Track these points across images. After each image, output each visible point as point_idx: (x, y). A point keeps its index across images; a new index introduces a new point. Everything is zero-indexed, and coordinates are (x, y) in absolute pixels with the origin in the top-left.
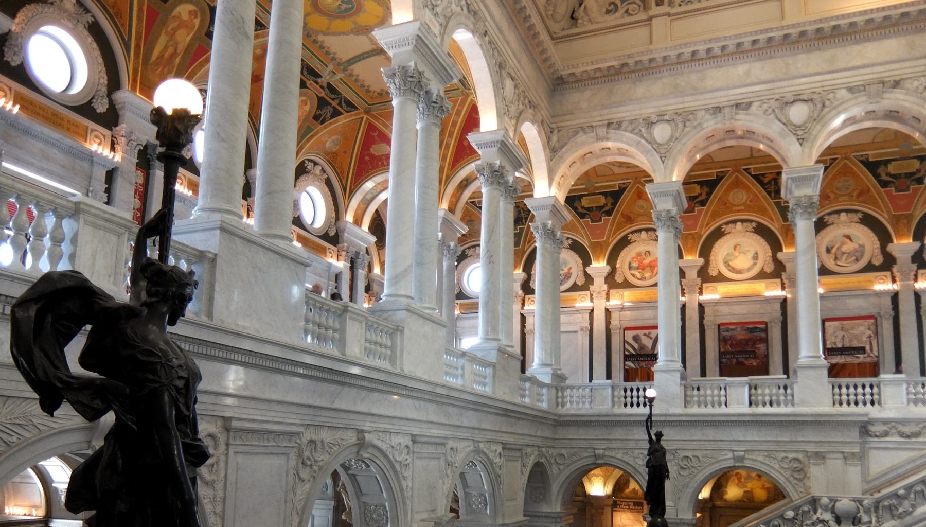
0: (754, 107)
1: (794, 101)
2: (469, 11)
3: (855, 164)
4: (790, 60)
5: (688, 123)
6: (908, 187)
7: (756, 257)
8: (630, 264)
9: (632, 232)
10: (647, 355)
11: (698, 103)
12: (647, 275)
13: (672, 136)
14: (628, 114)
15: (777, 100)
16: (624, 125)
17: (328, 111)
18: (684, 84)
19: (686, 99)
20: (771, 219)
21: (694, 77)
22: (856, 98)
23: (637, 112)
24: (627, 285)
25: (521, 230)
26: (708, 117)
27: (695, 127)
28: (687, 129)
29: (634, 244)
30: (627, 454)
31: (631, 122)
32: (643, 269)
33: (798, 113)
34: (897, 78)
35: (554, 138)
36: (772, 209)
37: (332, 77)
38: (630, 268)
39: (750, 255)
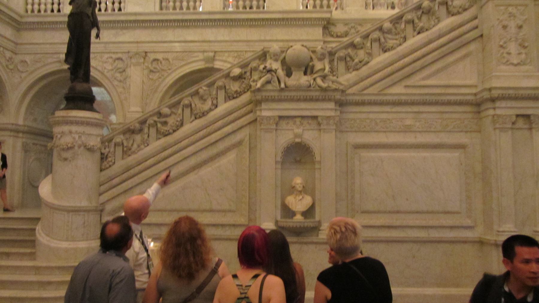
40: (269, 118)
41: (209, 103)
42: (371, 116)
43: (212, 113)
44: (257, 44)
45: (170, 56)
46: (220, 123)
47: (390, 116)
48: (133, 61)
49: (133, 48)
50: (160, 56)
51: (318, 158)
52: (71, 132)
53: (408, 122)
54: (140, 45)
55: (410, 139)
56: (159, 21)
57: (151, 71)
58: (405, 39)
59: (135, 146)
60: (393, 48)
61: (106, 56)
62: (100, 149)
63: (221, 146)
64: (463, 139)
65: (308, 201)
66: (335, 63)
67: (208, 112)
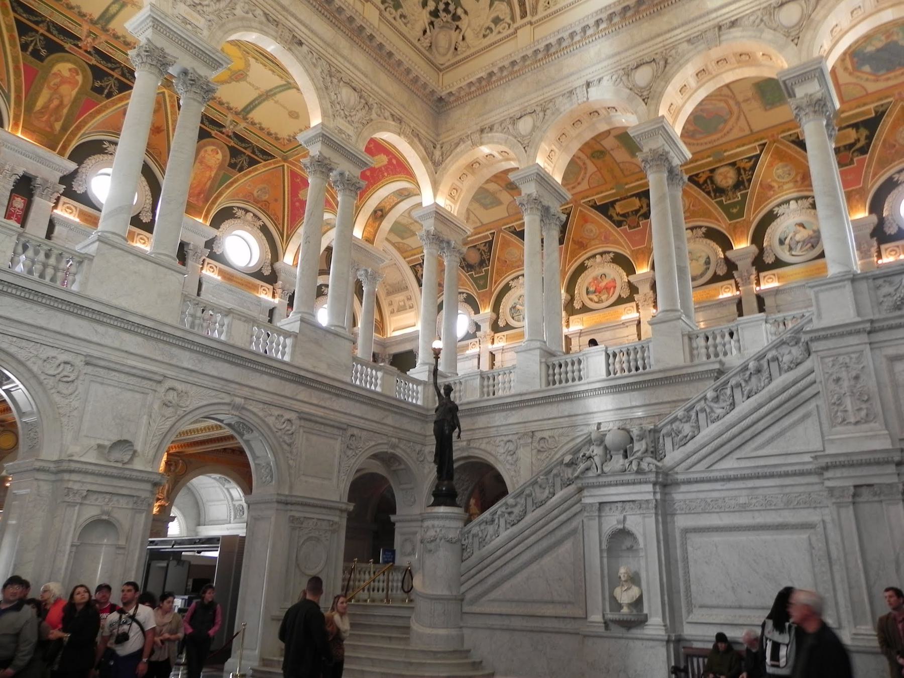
0: (605, 79)
3: (787, 146)
6: (852, 160)
7: (708, 262)
8: (587, 289)
9: (588, 259)
12: (604, 297)
14: (498, 117)
17: (243, 160)
19: (545, 90)
20: (717, 220)
22: (696, 47)
23: (505, 113)
24: (585, 309)
25: (487, 271)
27: (553, 114)
30: (488, 443)
31: (501, 123)
34: (733, 19)
35: (437, 153)
36: (716, 209)
37: (235, 126)
38: (588, 293)
39: (702, 261)
40: (591, 505)
41: (547, 491)
42: (702, 496)
45: (556, 433)
46: (556, 512)
47: (724, 494)
49: (521, 429)
50: (546, 434)
51: (642, 545)
52: (433, 526)
53: (742, 500)
54: (527, 425)
55: (745, 519)
56: (542, 398)
57: (539, 451)
58: (733, 405)
59: (488, 537)
60: (718, 418)
61: (499, 439)
62: (459, 540)
64: (813, 516)
65: (635, 592)
66: (661, 441)
67: (548, 498)
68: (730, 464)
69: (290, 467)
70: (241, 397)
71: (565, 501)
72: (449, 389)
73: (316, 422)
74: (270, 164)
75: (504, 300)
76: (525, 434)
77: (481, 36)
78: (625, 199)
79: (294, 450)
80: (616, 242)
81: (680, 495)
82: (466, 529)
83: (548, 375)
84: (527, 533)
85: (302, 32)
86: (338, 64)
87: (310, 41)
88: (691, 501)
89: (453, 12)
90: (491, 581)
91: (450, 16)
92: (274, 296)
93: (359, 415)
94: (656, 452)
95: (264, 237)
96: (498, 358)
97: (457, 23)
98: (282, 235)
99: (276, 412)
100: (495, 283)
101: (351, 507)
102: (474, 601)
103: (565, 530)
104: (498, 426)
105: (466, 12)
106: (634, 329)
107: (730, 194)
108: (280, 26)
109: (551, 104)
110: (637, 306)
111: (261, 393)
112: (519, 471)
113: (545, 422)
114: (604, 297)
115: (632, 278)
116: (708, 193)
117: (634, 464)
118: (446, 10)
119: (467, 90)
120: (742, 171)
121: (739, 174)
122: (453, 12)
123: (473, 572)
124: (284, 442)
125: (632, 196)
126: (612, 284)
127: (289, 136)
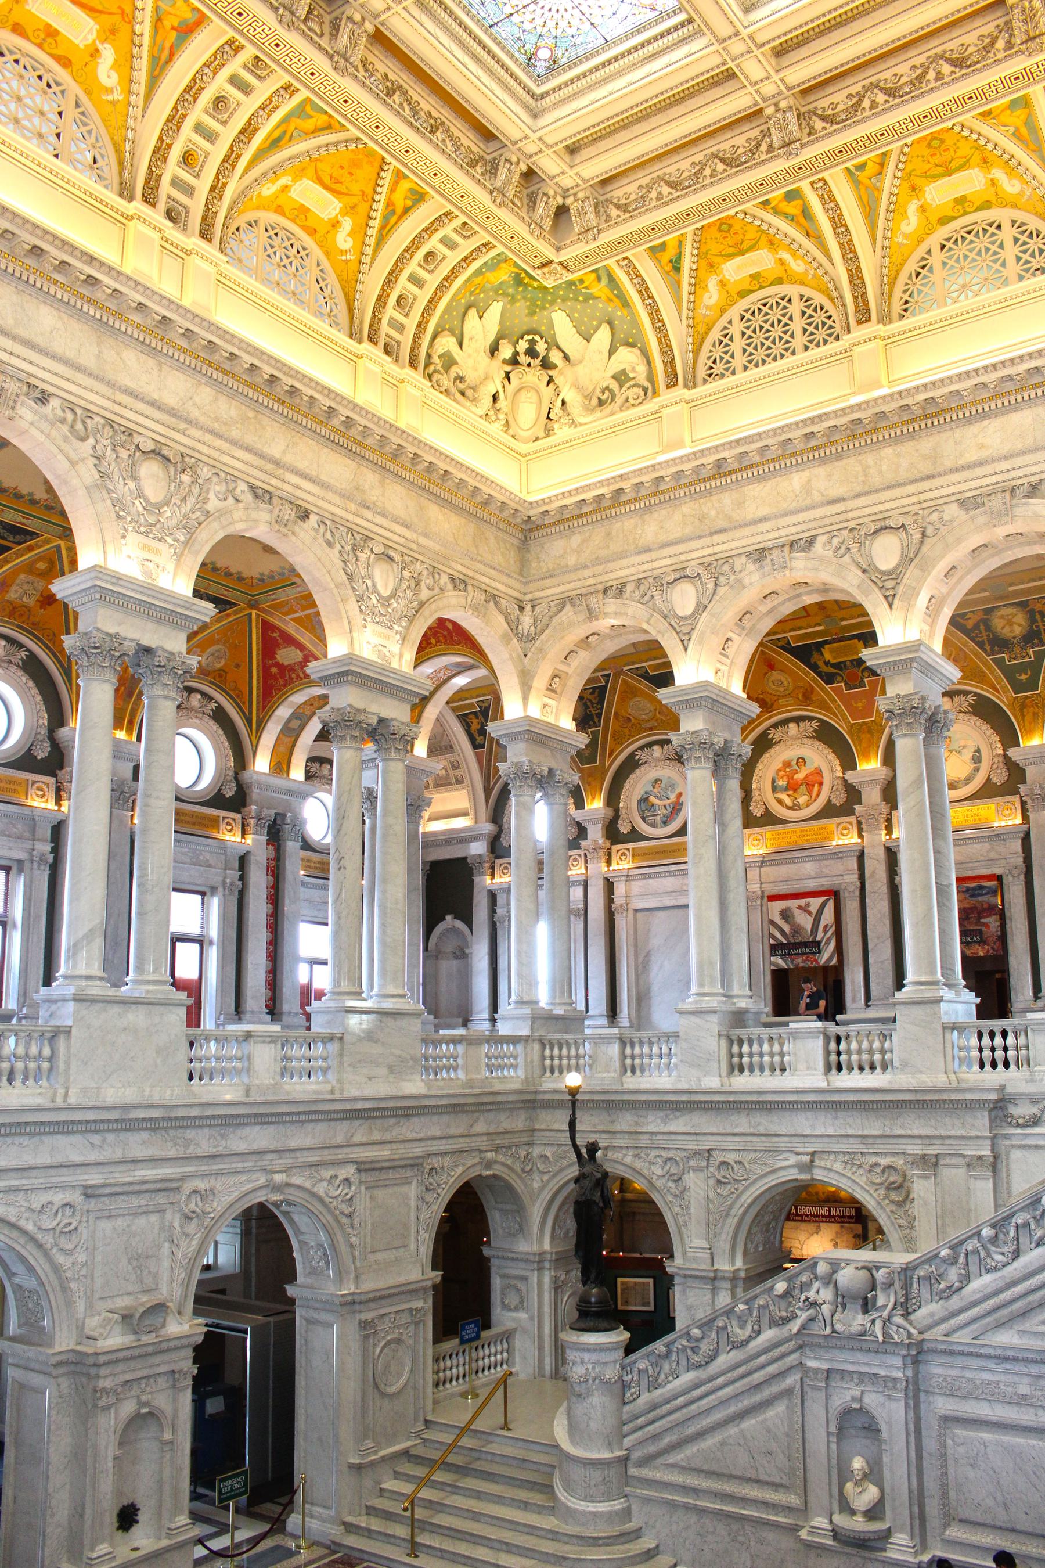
0: (821, 540)
1: (876, 532)
2: (256, 496)
4: (870, 459)
5: (722, 579)
7: (977, 759)
8: (773, 781)
10: (805, 945)
11: (734, 545)
12: (802, 800)
13: (699, 604)
14: (633, 570)
15: (852, 530)
16: (629, 588)
18: (713, 513)
21: (727, 499)
23: (646, 567)
24: (769, 819)
26: (751, 567)
28: (721, 591)
29: (777, 747)
31: (639, 583)
32: (795, 790)
33: (886, 552)
34: (1034, 479)
35: (527, 620)
38: (774, 789)
39: (968, 754)
40: (816, 1371)
42: (968, 1374)
43: (753, 1344)
44: (879, 1141)
46: (762, 1359)
47: (997, 1378)
48: (692, 1163)
50: (731, 1158)
51: (885, 1435)
52: (582, 1362)
57: (719, 1182)
58: (1017, 1254)
59: (662, 1376)
63: (766, 1393)
65: (872, 1492)
66: (915, 1285)
67: (750, 1338)
68: (1007, 1338)
69: (352, 1246)
70: (281, 1172)
71: (777, 1345)
72: (593, 1148)
73: (381, 1169)
74: (228, 615)
75: (627, 786)
76: (697, 1153)
77: (595, 401)
78: (840, 640)
79: (356, 1222)
80: (824, 706)
81: (937, 1370)
82: (628, 1360)
83: (732, 1056)
84: (720, 1380)
85: (308, 493)
86: (365, 524)
87: (320, 503)
88: (953, 1378)
89: (543, 353)
90: (666, 1440)
91: (538, 361)
92: (244, 833)
93: (438, 1134)
94: (906, 1308)
95: (220, 732)
96: (620, 889)
97: (551, 373)
98: (249, 721)
99: (327, 1174)
100: (610, 755)
101: (437, 1276)
102: (646, 1461)
103: (774, 1389)
104: (652, 1133)
105: (566, 357)
106: (853, 864)
107: (1017, 649)
108: (275, 500)
109: (726, 567)
110: (859, 823)
111: (305, 1153)
112: (688, 1208)
113: (730, 1138)
114: (802, 800)
115: (850, 776)
116: (981, 645)
117: (879, 1324)
118: (531, 352)
119: (577, 512)
120: (1038, 617)
121: (1033, 620)
122: (543, 353)
123: (641, 1421)
124: (342, 1213)
125: (853, 637)
126: (818, 778)
127: (262, 574)
